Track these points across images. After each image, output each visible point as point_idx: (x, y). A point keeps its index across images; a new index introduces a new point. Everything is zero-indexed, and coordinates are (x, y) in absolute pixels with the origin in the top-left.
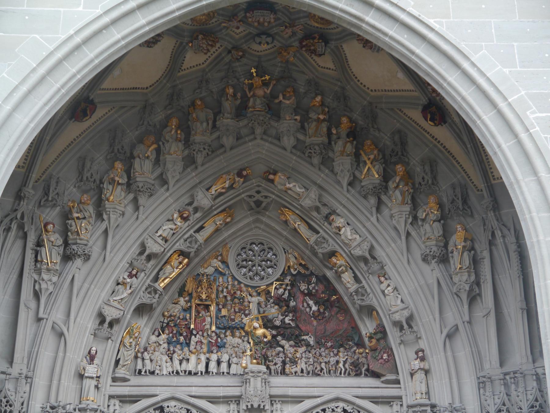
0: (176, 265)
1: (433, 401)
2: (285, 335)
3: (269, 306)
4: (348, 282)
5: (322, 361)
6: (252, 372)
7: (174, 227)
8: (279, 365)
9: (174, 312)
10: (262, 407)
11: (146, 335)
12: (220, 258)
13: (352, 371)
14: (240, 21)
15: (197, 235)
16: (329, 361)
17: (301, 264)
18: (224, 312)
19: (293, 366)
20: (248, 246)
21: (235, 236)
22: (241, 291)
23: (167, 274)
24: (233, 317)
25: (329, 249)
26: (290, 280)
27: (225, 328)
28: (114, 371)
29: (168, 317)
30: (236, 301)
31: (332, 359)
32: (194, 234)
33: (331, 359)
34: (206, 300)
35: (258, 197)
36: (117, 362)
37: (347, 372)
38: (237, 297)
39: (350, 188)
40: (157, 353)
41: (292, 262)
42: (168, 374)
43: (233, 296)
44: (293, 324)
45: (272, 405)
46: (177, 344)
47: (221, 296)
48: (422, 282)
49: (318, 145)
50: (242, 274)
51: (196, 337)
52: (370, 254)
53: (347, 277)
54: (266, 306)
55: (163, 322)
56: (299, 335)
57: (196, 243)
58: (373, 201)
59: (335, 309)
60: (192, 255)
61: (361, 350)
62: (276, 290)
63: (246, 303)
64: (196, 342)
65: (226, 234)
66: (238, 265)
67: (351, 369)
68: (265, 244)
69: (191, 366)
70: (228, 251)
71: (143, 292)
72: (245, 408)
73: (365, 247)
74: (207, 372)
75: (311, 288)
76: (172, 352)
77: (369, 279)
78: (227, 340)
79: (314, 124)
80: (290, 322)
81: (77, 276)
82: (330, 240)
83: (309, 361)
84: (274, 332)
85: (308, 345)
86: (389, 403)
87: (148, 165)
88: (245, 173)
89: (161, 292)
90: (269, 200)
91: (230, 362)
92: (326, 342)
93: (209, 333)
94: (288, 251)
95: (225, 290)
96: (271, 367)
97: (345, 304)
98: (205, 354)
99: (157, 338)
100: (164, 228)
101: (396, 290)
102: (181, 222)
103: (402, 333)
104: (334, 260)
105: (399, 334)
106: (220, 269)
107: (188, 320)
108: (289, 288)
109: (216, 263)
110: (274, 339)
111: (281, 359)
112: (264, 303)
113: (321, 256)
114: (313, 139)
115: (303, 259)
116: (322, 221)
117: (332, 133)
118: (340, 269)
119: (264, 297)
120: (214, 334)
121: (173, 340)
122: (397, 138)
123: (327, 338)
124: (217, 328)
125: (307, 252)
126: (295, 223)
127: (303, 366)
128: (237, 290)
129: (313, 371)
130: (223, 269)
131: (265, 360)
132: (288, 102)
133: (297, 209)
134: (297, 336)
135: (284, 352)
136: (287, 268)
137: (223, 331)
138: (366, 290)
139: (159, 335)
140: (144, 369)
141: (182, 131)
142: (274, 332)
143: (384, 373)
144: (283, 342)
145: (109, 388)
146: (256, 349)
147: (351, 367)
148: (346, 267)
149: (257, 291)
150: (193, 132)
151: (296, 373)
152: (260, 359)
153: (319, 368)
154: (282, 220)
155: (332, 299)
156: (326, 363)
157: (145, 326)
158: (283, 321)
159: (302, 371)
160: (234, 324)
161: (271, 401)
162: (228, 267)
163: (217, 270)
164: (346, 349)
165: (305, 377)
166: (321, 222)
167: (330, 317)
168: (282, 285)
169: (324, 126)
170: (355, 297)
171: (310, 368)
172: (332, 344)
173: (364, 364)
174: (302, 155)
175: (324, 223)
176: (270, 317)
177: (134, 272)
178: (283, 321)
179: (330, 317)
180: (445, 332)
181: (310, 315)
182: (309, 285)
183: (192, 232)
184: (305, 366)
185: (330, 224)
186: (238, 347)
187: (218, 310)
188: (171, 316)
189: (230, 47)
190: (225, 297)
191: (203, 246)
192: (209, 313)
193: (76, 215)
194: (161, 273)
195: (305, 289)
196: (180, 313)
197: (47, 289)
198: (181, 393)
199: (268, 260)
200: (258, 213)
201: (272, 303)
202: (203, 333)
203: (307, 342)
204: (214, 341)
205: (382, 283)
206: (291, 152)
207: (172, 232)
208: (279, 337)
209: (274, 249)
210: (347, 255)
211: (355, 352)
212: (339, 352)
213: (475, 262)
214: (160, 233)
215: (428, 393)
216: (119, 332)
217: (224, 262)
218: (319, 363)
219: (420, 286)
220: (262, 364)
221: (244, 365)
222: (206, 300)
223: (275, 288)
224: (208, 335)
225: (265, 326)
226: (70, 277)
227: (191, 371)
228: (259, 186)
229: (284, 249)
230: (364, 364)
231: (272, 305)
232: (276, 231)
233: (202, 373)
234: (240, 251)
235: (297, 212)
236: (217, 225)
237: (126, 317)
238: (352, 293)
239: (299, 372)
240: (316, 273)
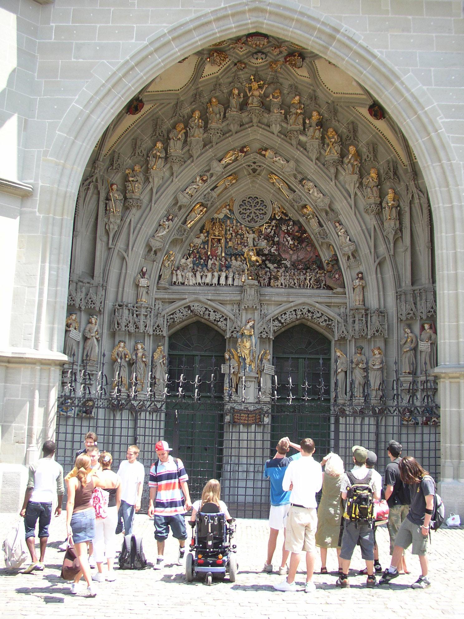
7: (197, 187)
11: (179, 258)
12: (228, 207)
14: (243, 44)
17: (282, 212)
18: (230, 244)
23: (192, 219)
27: (231, 255)
28: (158, 283)
30: (239, 236)
34: (219, 236)
36: (160, 276)
41: (277, 209)
43: (237, 233)
45: (261, 306)
47: (229, 233)
48: (364, 228)
49: (296, 131)
52: (329, 207)
53: (314, 223)
54: (259, 240)
58: (333, 170)
59: (305, 243)
61: (321, 272)
63: (245, 238)
69: (208, 280)
70: (233, 202)
72: (243, 308)
74: (219, 284)
79: (294, 116)
81: (133, 219)
82: (303, 197)
84: (264, 258)
85: (286, 267)
87: (179, 144)
88: (245, 150)
90: (262, 168)
95: (231, 229)
100: (190, 187)
104: (305, 210)
108: (274, 228)
109: (225, 211)
114: (292, 126)
115: (284, 209)
117: (306, 123)
119: (257, 234)
120: (223, 259)
122: (351, 126)
127: (283, 281)
131: (257, 277)
132: (276, 100)
133: (281, 175)
139: (187, 258)
141: (202, 120)
142: (264, 258)
144: (269, 265)
145: (155, 293)
150: (210, 121)
153: (293, 283)
159: (282, 285)
164: (311, 270)
168: (269, 226)
169: (301, 117)
174: (285, 138)
178: (270, 251)
180: (377, 261)
183: (209, 189)
188: (195, 246)
189: (236, 61)
190: (232, 234)
192: (219, 245)
193: (131, 179)
197: (114, 229)
198: (202, 298)
200: (254, 176)
206: (277, 136)
207: (196, 190)
210: (314, 208)
211: (317, 273)
212: (306, 272)
213: (400, 214)
214: (187, 190)
215: (364, 301)
216: (161, 257)
217: (230, 210)
221: (243, 280)
225: (258, 254)
226: (129, 220)
228: (255, 158)
232: (267, 189)
239: (279, 284)
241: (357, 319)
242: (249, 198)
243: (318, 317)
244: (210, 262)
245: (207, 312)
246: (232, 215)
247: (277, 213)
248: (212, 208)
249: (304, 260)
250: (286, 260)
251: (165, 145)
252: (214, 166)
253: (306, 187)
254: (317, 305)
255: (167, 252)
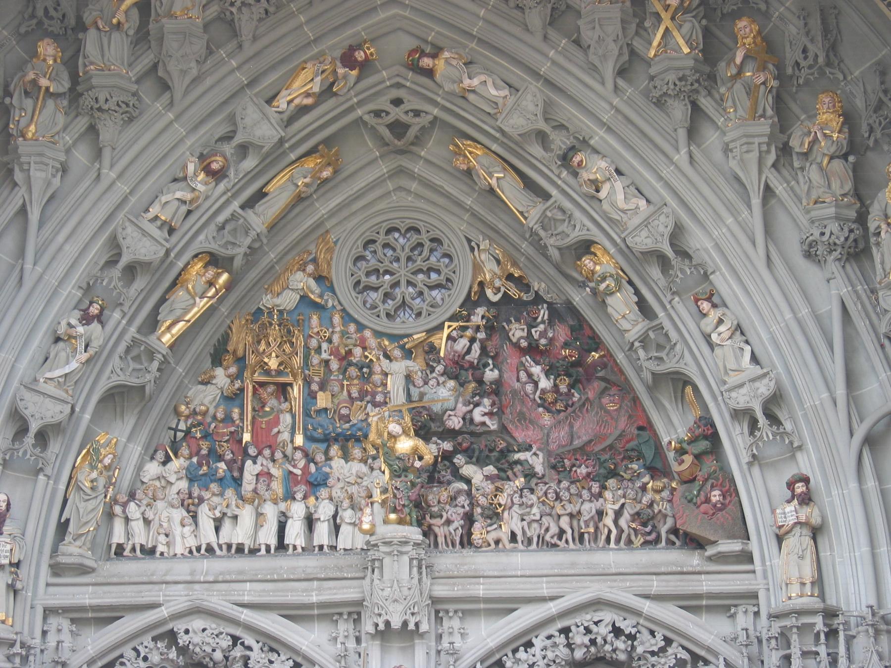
0: (199, 290)
1: (832, 601)
2: (474, 451)
3: (432, 382)
4: (623, 317)
5: (560, 512)
6: (385, 543)
8: (456, 524)
9: (202, 404)
10: (411, 626)
12: (310, 268)
13: (636, 536)
15: (250, 214)
16: (579, 512)
17: (510, 277)
18: (323, 400)
19: (491, 525)
20: (382, 238)
21: (345, 213)
22: (365, 348)
23: (178, 313)
24: (344, 411)
25: (575, 235)
26: (483, 317)
27: (327, 440)
29: (188, 417)
30: (353, 371)
31: (586, 506)
32: (240, 211)
33: (583, 507)
35: (397, 113)
37: (624, 536)
38: (354, 361)
39: (621, 82)
40: (160, 504)
41: (490, 269)
42: (186, 553)
44: (493, 425)
46: (212, 481)
47: (315, 360)
48: (804, 312)
50: (368, 306)
51: (255, 463)
54: (426, 383)
55: (176, 430)
56: (509, 451)
57: (247, 233)
59: (598, 385)
60: (238, 262)
61: (659, 484)
62: (449, 342)
63: (377, 378)
64: (257, 475)
65: (323, 208)
66: (358, 283)
67: (634, 529)
68: (423, 231)
70: (330, 250)
71: (121, 357)
73: (661, 229)
74: (282, 546)
75: (536, 336)
76: (196, 501)
77: (672, 307)
78: (331, 468)
80: (486, 419)
83: (529, 513)
84: (447, 446)
85: (530, 474)
86: (727, 608)
89: (164, 356)
91: (338, 521)
92: (574, 465)
93: (289, 450)
94: (478, 246)
95: (325, 346)
96: (436, 529)
97: (621, 372)
98: (275, 503)
99: (161, 468)
100: (164, 199)
101: (738, 333)
102: (206, 184)
103: (755, 436)
105: (750, 440)
106: (312, 297)
107: (237, 422)
108: (481, 335)
109: (301, 281)
110: (446, 463)
111: (461, 511)
112: (419, 373)
113: (554, 254)
115: (515, 264)
116: (554, 168)
118: (603, 286)
120: (299, 455)
121: (201, 472)
123: (578, 456)
124: (309, 438)
125: (524, 245)
126: (491, 177)
128: (355, 345)
129: (539, 537)
130: (321, 296)
134: (501, 451)
135: (469, 494)
136: (476, 288)
137: (323, 446)
138: (666, 335)
139: (167, 460)
140: (130, 542)
142: (447, 446)
143: (712, 539)
144: (468, 470)
146: (396, 488)
147: (634, 526)
148: (618, 281)
149: (402, 347)
151: (497, 542)
152: (407, 510)
153: (554, 529)
154: (457, 169)
155: (590, 360)
156: (571, 516)
157: (129, 439)
158: (468, 417)
159: (513, 537)
160: (348, 430)
161: (437, 612)
162: (332, 289)
163: (304, 298)
165: (522, 551)
166: (552, 172)
167: (584, 404)
170: (641, 353)
171: (534, 531)
172: (590, 470)
173: (665, 516)
175: (561, 173)
176: (437, 408)
177: (94, 310)
178: (467, 419)
179: (584, 404)
180: (860, 433)
181: (535, 400)
182: (530, 326)
183: (235, 205)
184: (520, 524)
185: (575, 174)
186: (358, 484)
187: (309, 395)
188: (195, 413)
190: (327, 362)
191: (265, 241)
192: (285, 406)
194: (164, 310)
195: (522, 337)
196: (216, 407)
199: (430, 269)
200: (402, 152)
201: (442, 375)
202: (273, 454)
203: (527, 467)
204: (299, 472)
205: (705, 315)
207: (184, 209)
208: (459, 456)
209: (446, 242)
210: (621, 251)
211: (644, 488)
212: (604, 487)
214: (154, 210)
215: (819, 582)
217: (319, 279)
218: (556, 517)
219: (799, 322)
220: (411, 524)
222: (279, 373)
223: (449, 337)
224: (285, 456)
225: (423, 432)
227: (243, 544)
229: (469, 241)
230: (665, 516)
231: (441, 379)
233: (268, 550)
234: (361, 249)
235: (494, 147)
236: (298, 186)
237: (79, 419)
238: (632, 344)
240: (547, 297)
241: (795, 652)
242: (389, 231)
243: (653, 653)
244: (251, 469)
245: (238, 652)
246: (328, 295)
247: (492, 282)
248: (253, 275)
249: (597, 448)
250: (529, 448)
251: (69, 54)
252: (248, 121)
253: (585, 175)
254: (647, 607)
255: (88, 438)
